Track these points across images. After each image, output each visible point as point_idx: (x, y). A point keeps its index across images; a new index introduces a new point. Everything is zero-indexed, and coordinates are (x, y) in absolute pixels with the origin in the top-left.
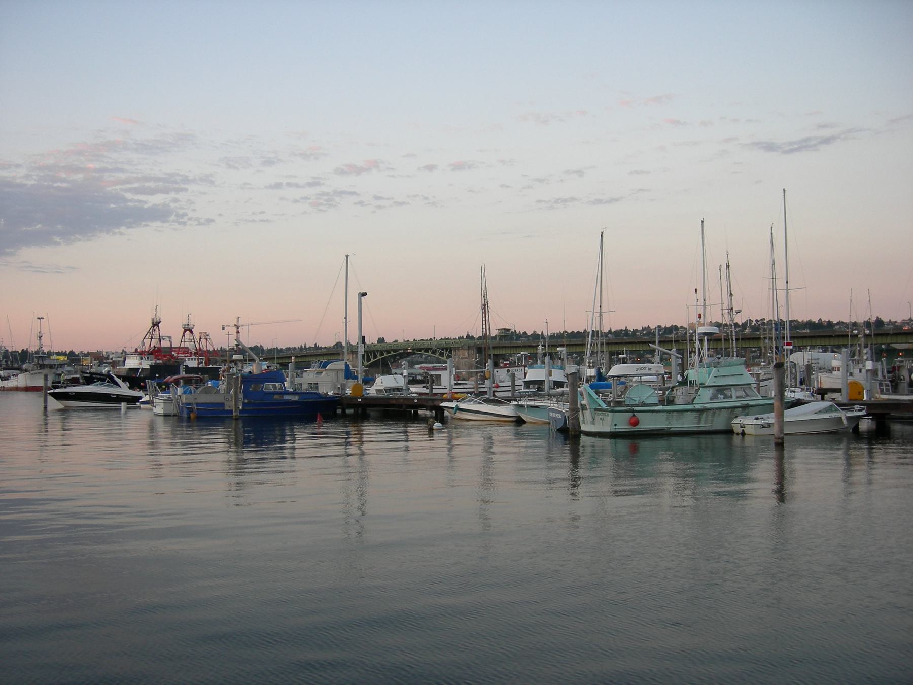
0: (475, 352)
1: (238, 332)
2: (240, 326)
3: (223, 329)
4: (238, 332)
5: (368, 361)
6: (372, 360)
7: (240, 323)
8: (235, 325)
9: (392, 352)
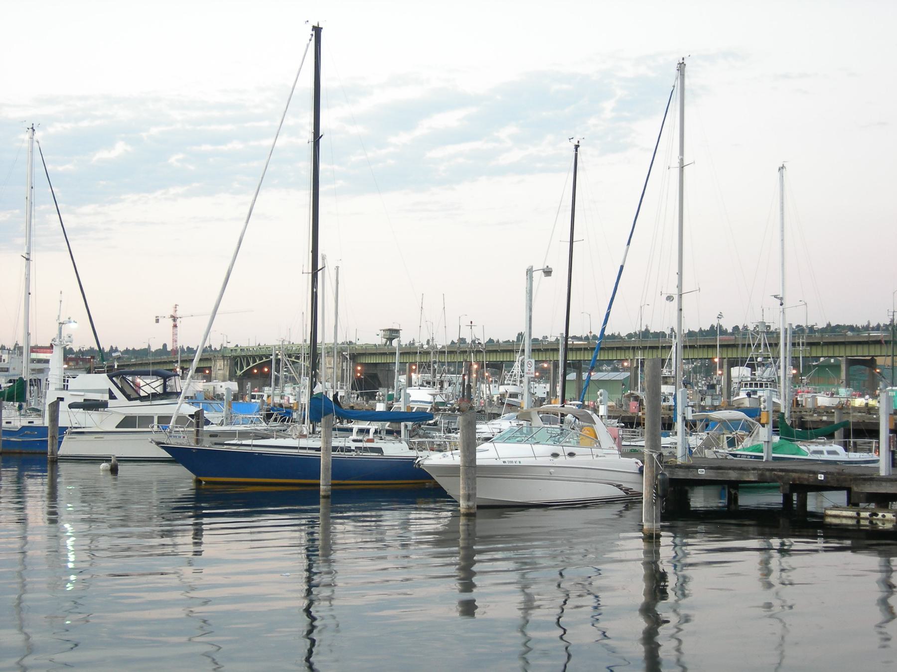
0: (341, 361)
1: (175, 326)
2: (178, 318)
3: (157, 321)
4: (175, 326)
5: (241, 370)
6: (245, 369)
7: (178, 314)
8: (172, 316)
9: (264, 358)
